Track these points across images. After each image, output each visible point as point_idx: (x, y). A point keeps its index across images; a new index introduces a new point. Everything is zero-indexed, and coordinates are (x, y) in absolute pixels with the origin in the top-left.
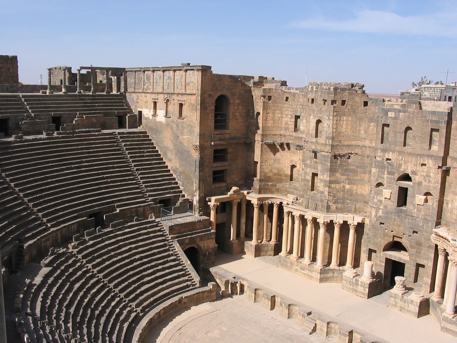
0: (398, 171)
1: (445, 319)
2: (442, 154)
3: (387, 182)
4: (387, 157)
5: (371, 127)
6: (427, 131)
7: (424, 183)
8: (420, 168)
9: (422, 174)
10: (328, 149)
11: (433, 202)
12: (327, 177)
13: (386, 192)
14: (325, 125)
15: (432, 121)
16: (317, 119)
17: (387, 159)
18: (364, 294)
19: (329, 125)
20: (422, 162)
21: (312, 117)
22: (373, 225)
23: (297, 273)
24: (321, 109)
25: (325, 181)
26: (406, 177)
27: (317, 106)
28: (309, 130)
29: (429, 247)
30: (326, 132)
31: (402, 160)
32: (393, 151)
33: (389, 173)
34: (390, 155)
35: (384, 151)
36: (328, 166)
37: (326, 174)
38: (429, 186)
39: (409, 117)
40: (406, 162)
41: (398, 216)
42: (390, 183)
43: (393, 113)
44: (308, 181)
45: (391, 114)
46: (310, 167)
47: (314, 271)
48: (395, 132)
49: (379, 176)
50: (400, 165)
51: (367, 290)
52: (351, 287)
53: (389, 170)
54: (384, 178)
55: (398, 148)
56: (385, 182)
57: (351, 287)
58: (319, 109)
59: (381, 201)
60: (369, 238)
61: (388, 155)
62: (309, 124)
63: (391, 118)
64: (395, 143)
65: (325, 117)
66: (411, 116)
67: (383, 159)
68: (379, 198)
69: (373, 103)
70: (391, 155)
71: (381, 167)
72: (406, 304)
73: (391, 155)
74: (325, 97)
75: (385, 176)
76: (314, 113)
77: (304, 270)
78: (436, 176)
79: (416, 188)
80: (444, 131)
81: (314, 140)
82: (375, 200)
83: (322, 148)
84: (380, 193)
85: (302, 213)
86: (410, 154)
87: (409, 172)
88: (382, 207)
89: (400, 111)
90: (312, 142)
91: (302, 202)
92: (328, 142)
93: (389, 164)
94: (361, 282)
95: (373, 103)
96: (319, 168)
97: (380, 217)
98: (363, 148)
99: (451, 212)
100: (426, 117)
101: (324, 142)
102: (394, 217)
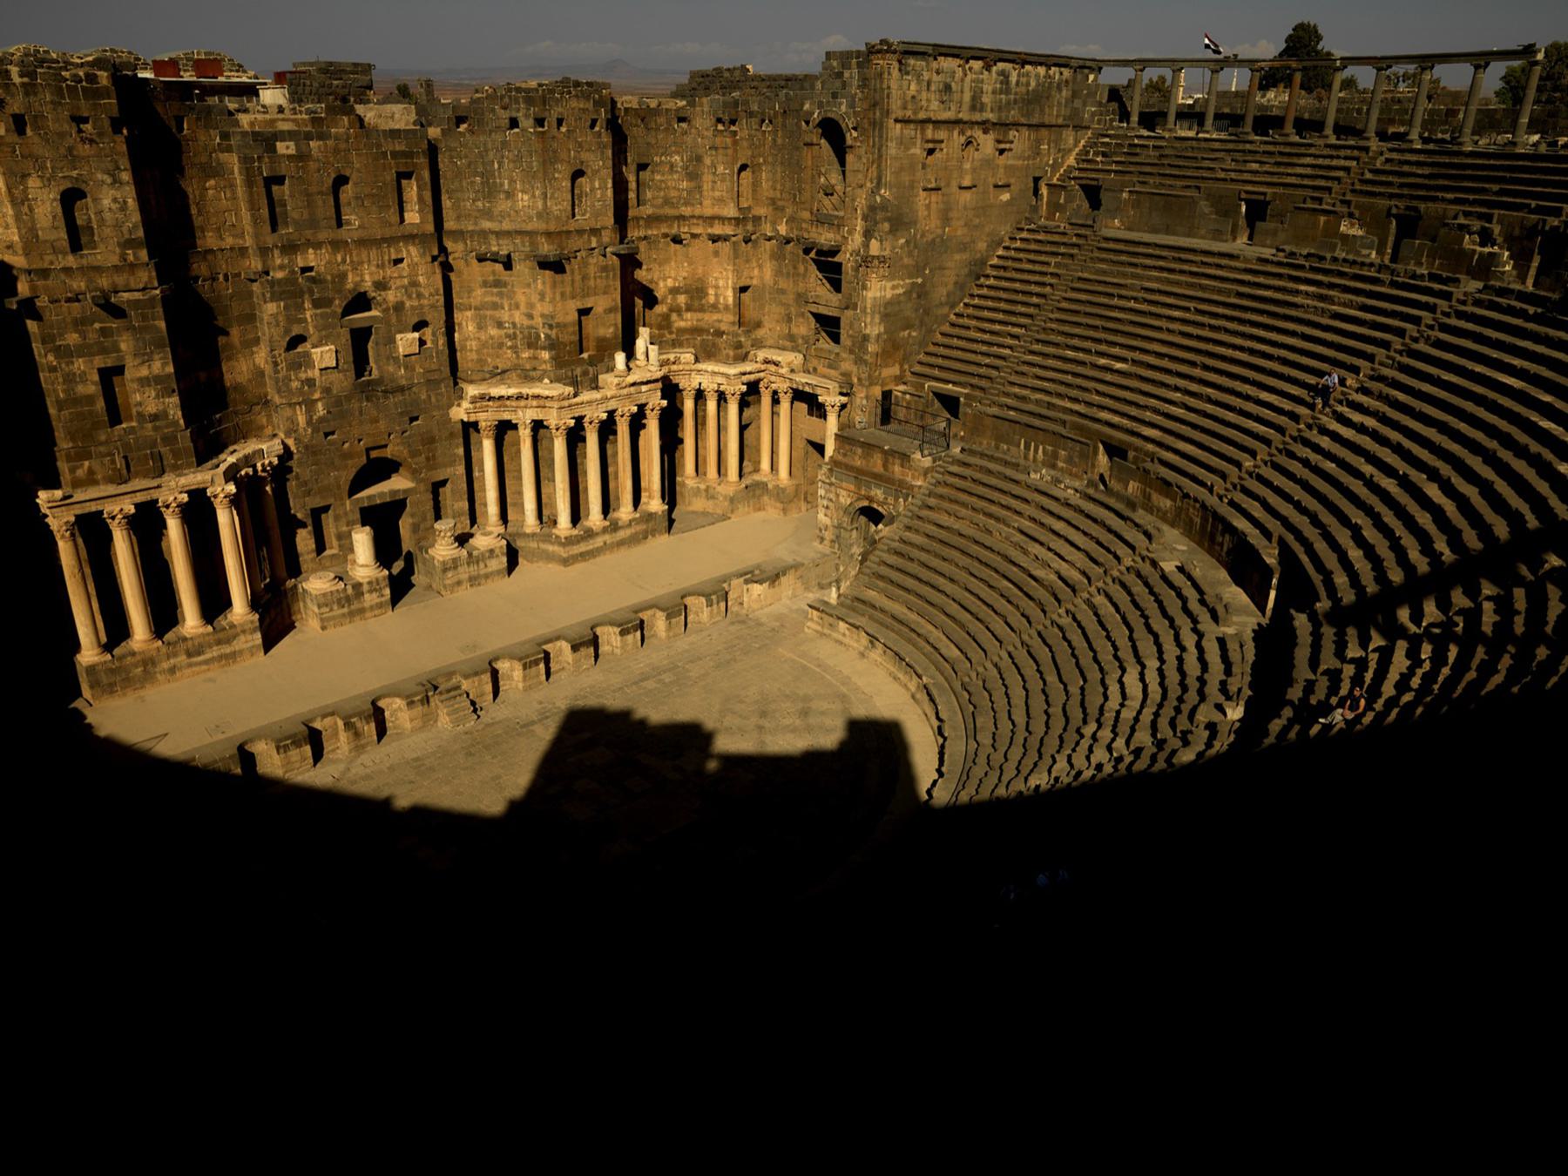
0: (339, 291)
1: (570, 541)
2: (430, 228)
3: (315, 327)
4: (301, 264)
5: (211, 192)
6: (388, 178)
7: (408, 304)
8: (390, 271)
9: (399, 283)
10: (145, 279)
11: (434, 336)
12: (164, 365)
13: (323, 355)
14: (106, 202)
15: (395, 154)
16: (62, 188)
17: (305, 270)
18: (380, 606)
19: (125, 202)
20: (394, 257)
21: (33, 182)
22: (306, 447)
23: (178, 674)
24: (70, 149)
25: (158, 379)
26: (361, 302)
27: (47, 141)
28: (33, 230)
29: (452, 435)
30: (118, 226)
31: (344, 261)
32: (317, 246)
33: (317, 304)
34: (311, 258)
35: (290, 248)
36: (158, 330)
37: (156, 357)
38: (422, 306)
39: (336, 151)
40: (356, 266)
41: (368, 399)
42: (325, 328)
43: (292, 144)
44: (90, 399)
45: (285, 148)
46: (83, 351)
47: (235, 636)
48: (308, 195)
49: (292, 320)
50: (343, 276)
51: (387, 591)
52: (346, 610)
53: (316, 296)
54: (305, 320)
55: (323, 235)
56: (311, 330)
57: (346, 610)
58: (63, 151)
59: (310, 382)
60: (306, 483)
61: (306, 259)
62: (31, 209)
63: (289, 157)
64: (313, 224)
65: (99, 176)
66: (343, 146)
67: (293, 272)
68: (303, 376)
69: (198, 119)
70: (312, 257)
71: (289, 292)
72: (482, 565)
73: (312, 257)
74: (79, 108)
75: (308, 314)
76: (43, 168)
77: (199, 654)
78: (430, 280)
79: (394, 320)
80: (426, 174)
81: (71, 261)
82: (295, 384)
83: (120, 280)
84: (307, 361)
85: (140, 498)
86: (363, 243)
87: (367, 285)
88: (317, 396)
89: (308, 137)
90: (67, 270)
91: (91, 472)
92: (131, 258)
93: (313, 280)
94: (370, 583)
95: (198, 119)
96: (123, 346)
97: (321, 420)
98: (209, 257)
99: (464, 348)
100: (379, 146)
101: (114, 260)
102: (357, 405)
